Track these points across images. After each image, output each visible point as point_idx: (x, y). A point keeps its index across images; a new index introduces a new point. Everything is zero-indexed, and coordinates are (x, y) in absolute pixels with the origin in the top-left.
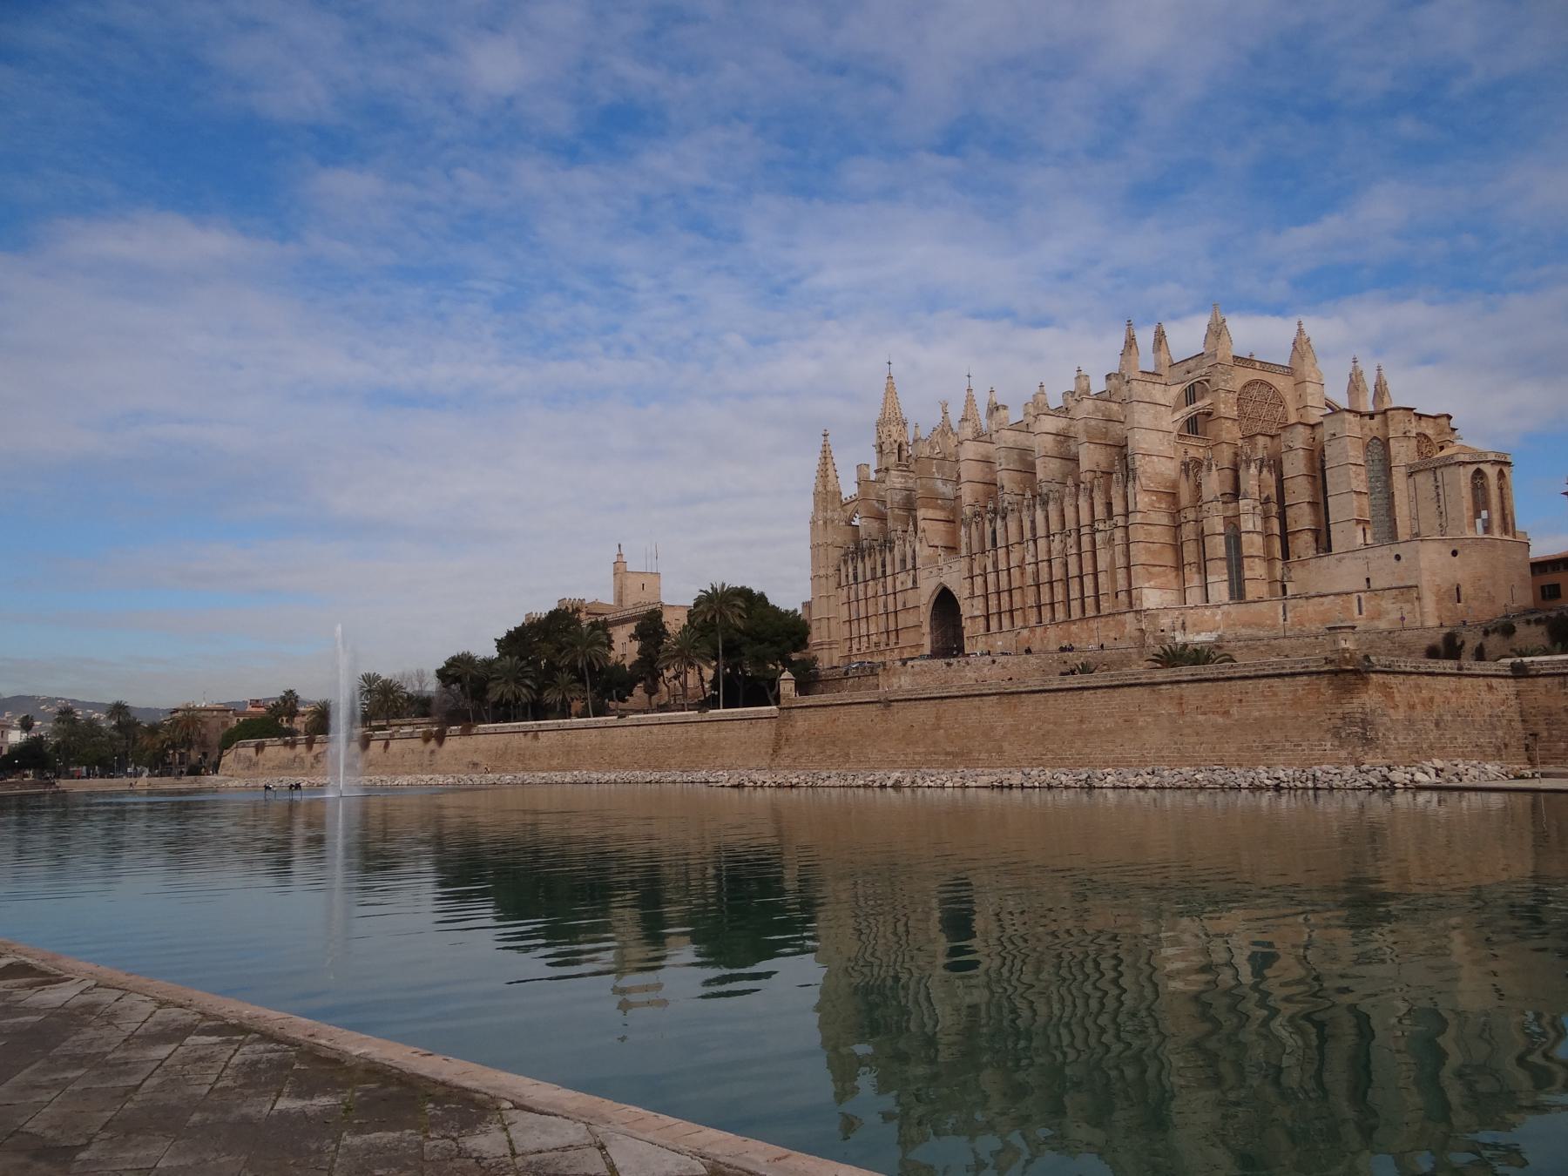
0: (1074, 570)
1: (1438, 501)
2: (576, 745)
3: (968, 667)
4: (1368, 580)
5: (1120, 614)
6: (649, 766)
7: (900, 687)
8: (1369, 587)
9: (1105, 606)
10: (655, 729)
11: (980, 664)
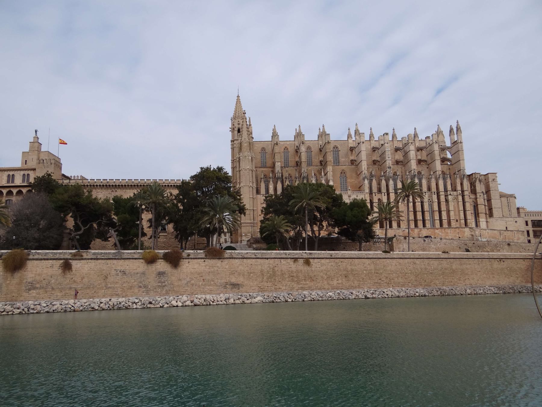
0: (436, 207)
1: (509, 207)
2: (352, 270)
3: (432, 243)
4: (506, 227)
5: (462, 228)
6: (421, 285)
7: (404, 249)
8: (507, 229)
9: (453, 224)
10: (418, 261)
11: (436, 241)
